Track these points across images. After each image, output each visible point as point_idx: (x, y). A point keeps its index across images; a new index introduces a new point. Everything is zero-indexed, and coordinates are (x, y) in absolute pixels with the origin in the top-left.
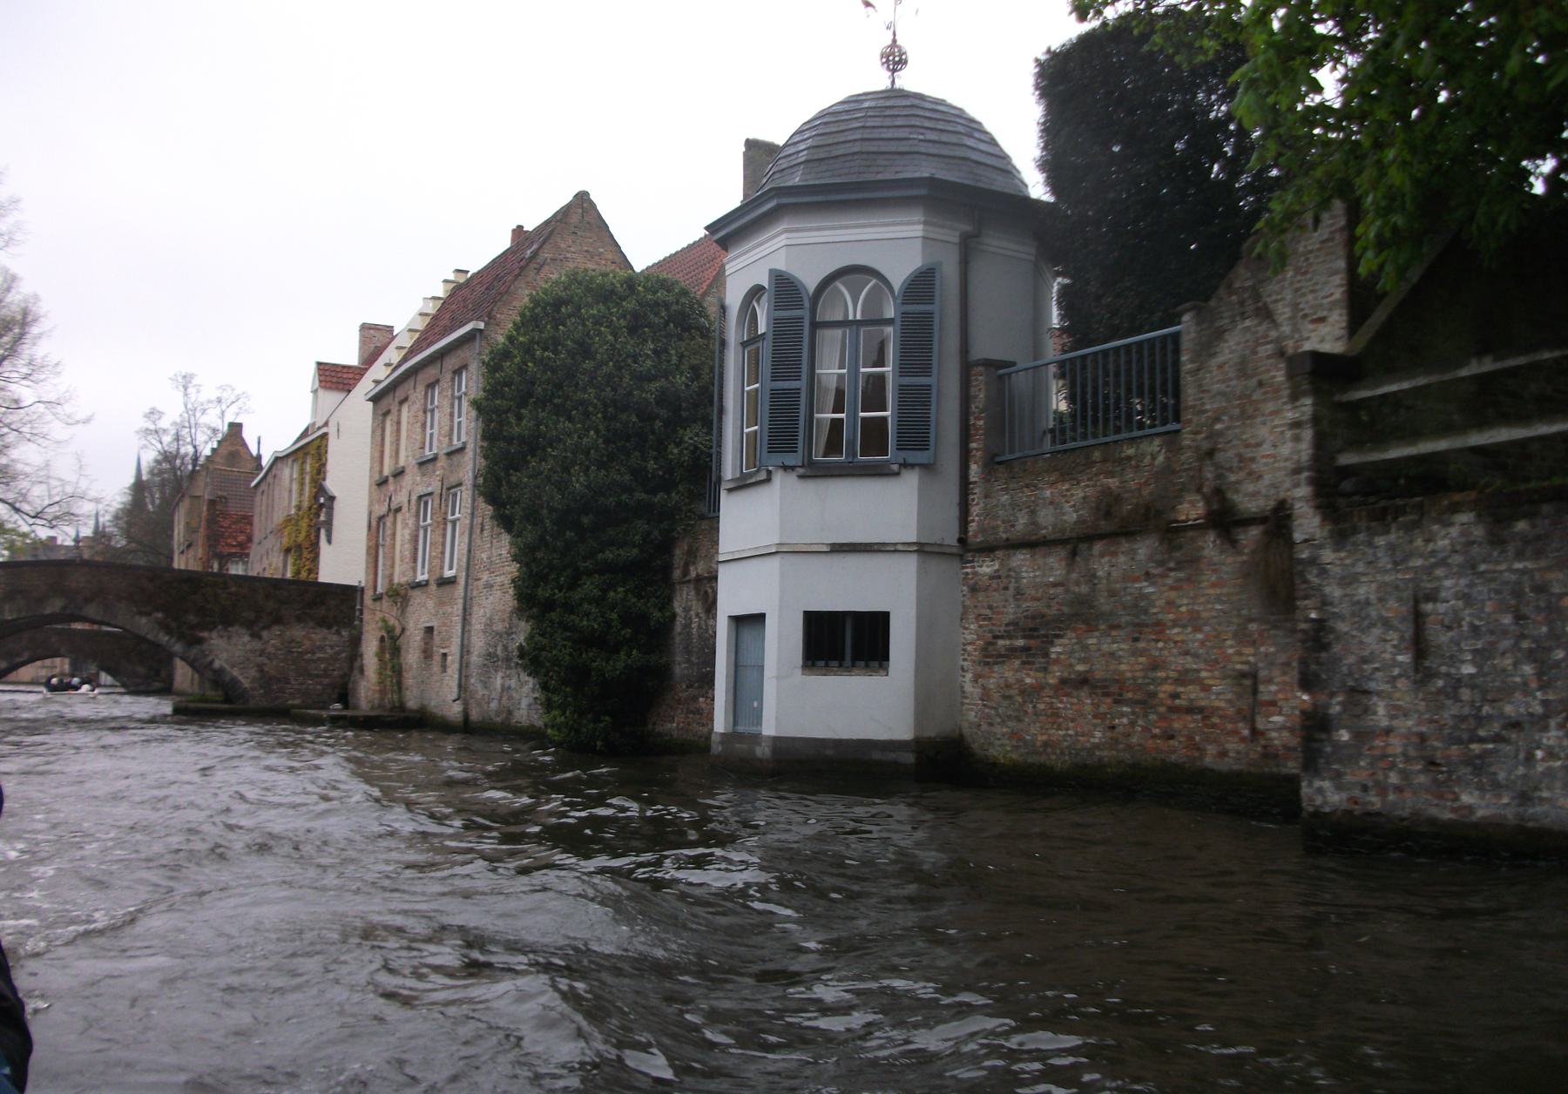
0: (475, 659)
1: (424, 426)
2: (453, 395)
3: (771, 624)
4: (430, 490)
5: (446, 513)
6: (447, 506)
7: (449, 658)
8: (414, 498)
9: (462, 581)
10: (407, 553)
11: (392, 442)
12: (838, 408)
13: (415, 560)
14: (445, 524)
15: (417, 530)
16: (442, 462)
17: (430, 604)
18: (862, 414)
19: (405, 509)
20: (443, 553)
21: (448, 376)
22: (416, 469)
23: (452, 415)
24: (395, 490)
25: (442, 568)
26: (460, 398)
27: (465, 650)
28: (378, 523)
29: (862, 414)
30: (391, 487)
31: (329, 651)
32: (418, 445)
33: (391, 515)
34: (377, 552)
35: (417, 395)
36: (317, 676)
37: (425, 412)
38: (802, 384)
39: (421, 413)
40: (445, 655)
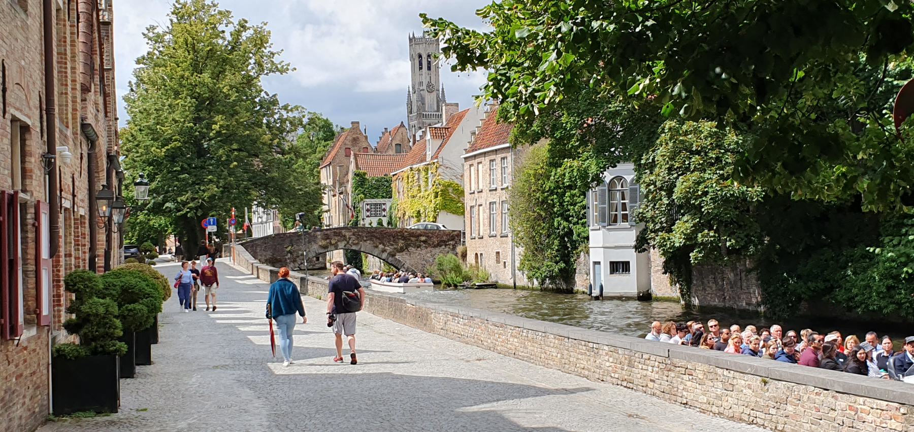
1: (490, 175)
3: (602, 263)
4: (494, 200)
8: (488, 203)
11: (475, 178)
12: (616, 211)
13: (490, 226)
17: (498, 243)
18: (622, 212)
19: (484, 205)
20: (502, 225)
26: (504, 168)
27: (513, 262)
29: (622, 212)
30: (476, 194)
35: (486, 160)
37: (490, 170)
38: (606, 206)
39: (488, 170)
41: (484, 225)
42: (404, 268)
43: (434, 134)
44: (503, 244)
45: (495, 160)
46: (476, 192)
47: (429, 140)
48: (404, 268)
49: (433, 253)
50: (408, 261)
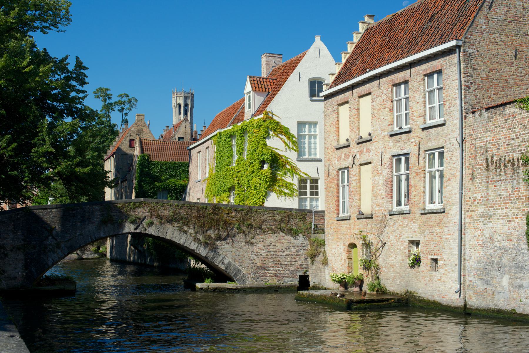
0: (470, 264)
1: (391, 110)
2: (424, 90)
4: (405, 151)
5: (425, 167)
6: (425, 162)
7: (440, 263)
8: (387, 157)
9: (454, 210)
10: (383, 193)
11: (351, 122)
13: (392, 197)
14: (425, 174)
15: (392, 178)
16: (417, 132)
17: (415, 226)
20: (424, 192)
21: (419, 78)
22: (387, 138)
23: (424, 102)
24: (361, 152)
25: (424, 203)
28: (338, 173)
30: (354, 149)
31: (293, 250)
32: (387, 123)
33: (355, 169)
34: (338, 190)
36: (286, 265)
39: (389, 102)
40: (435, 261)
41: (375, 196)
42: (223, 263)
43: (257, 85)
44: (431, 226)
45: (406, 82)
46: (353, 144)
47: (250, 92)
48: (223, 263)
49: (267, 242)
50: (229, 254)
